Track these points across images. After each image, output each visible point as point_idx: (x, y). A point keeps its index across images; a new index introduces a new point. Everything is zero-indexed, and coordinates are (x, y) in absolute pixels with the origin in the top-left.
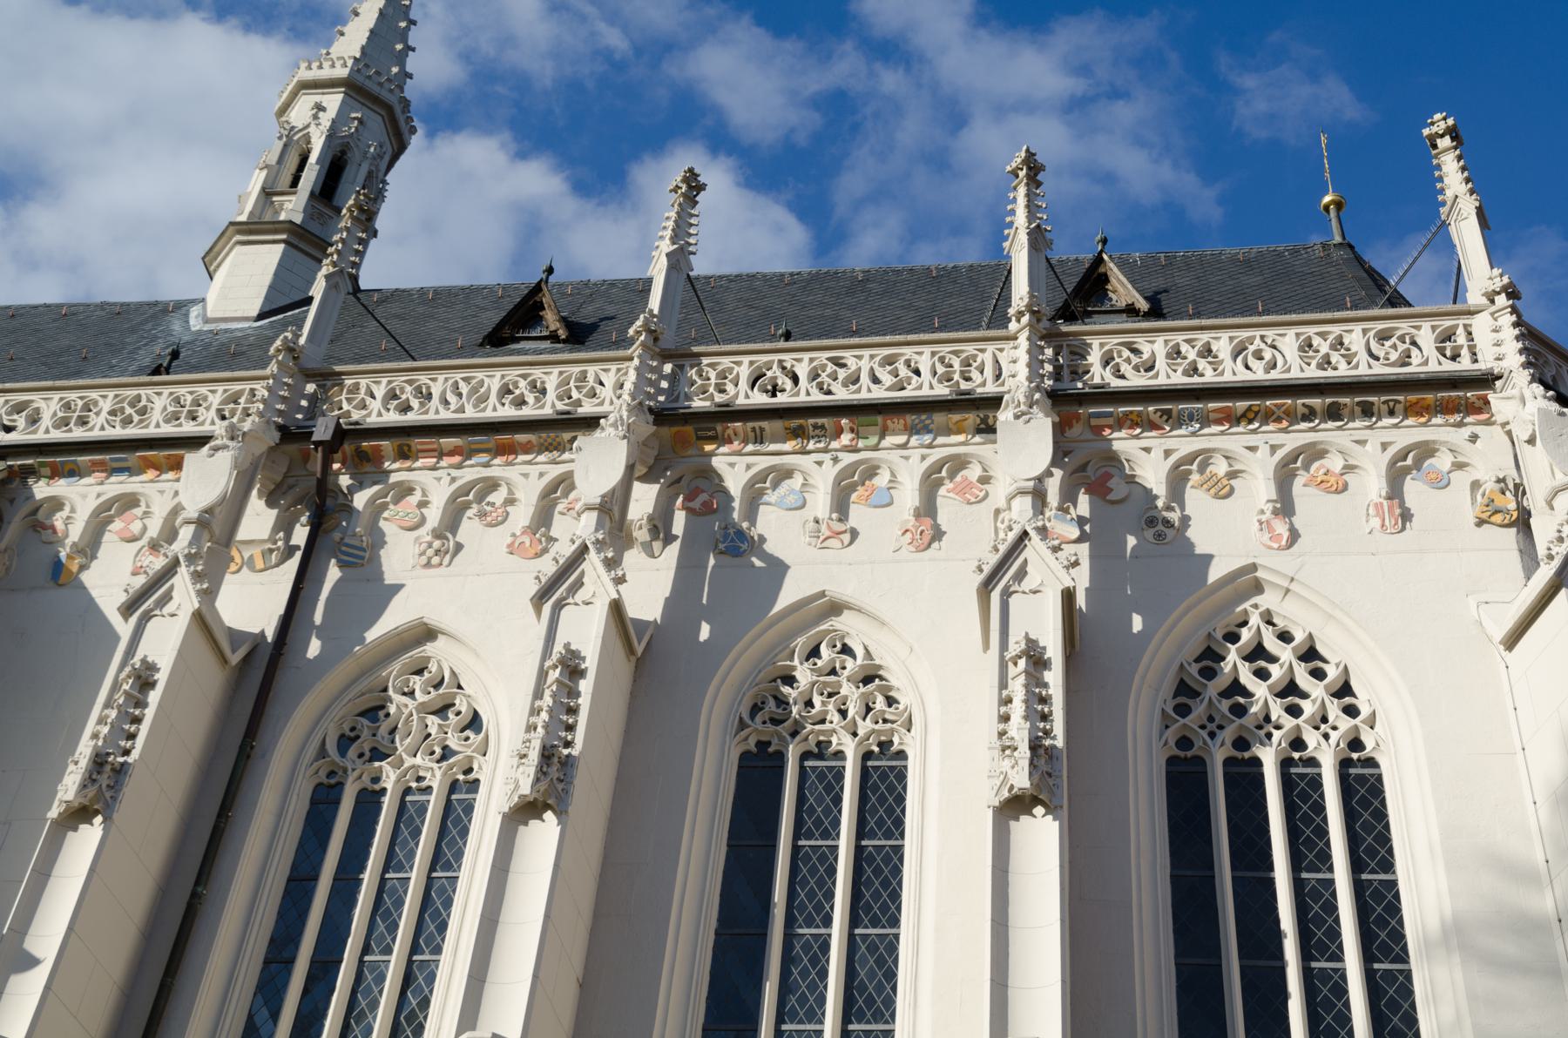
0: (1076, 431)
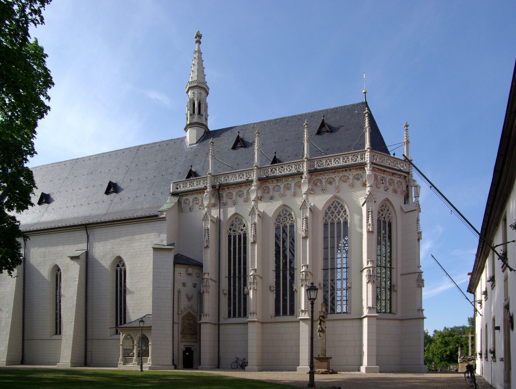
0: (313, 176)
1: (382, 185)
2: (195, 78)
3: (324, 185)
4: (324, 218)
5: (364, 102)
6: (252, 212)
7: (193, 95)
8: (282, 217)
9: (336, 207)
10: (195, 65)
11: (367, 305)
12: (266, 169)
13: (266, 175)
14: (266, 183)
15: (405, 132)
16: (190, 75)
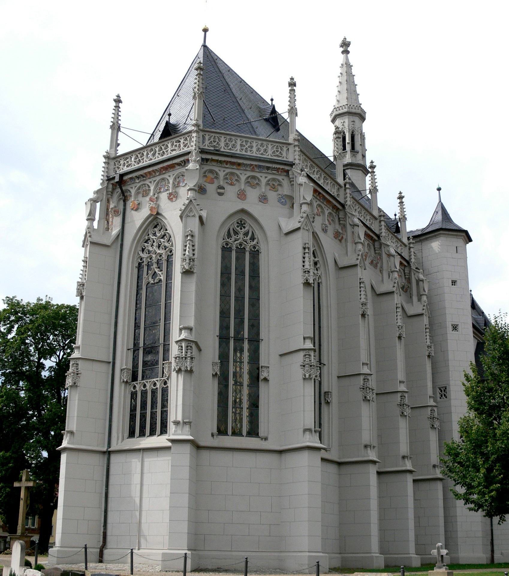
2: (345, 102)
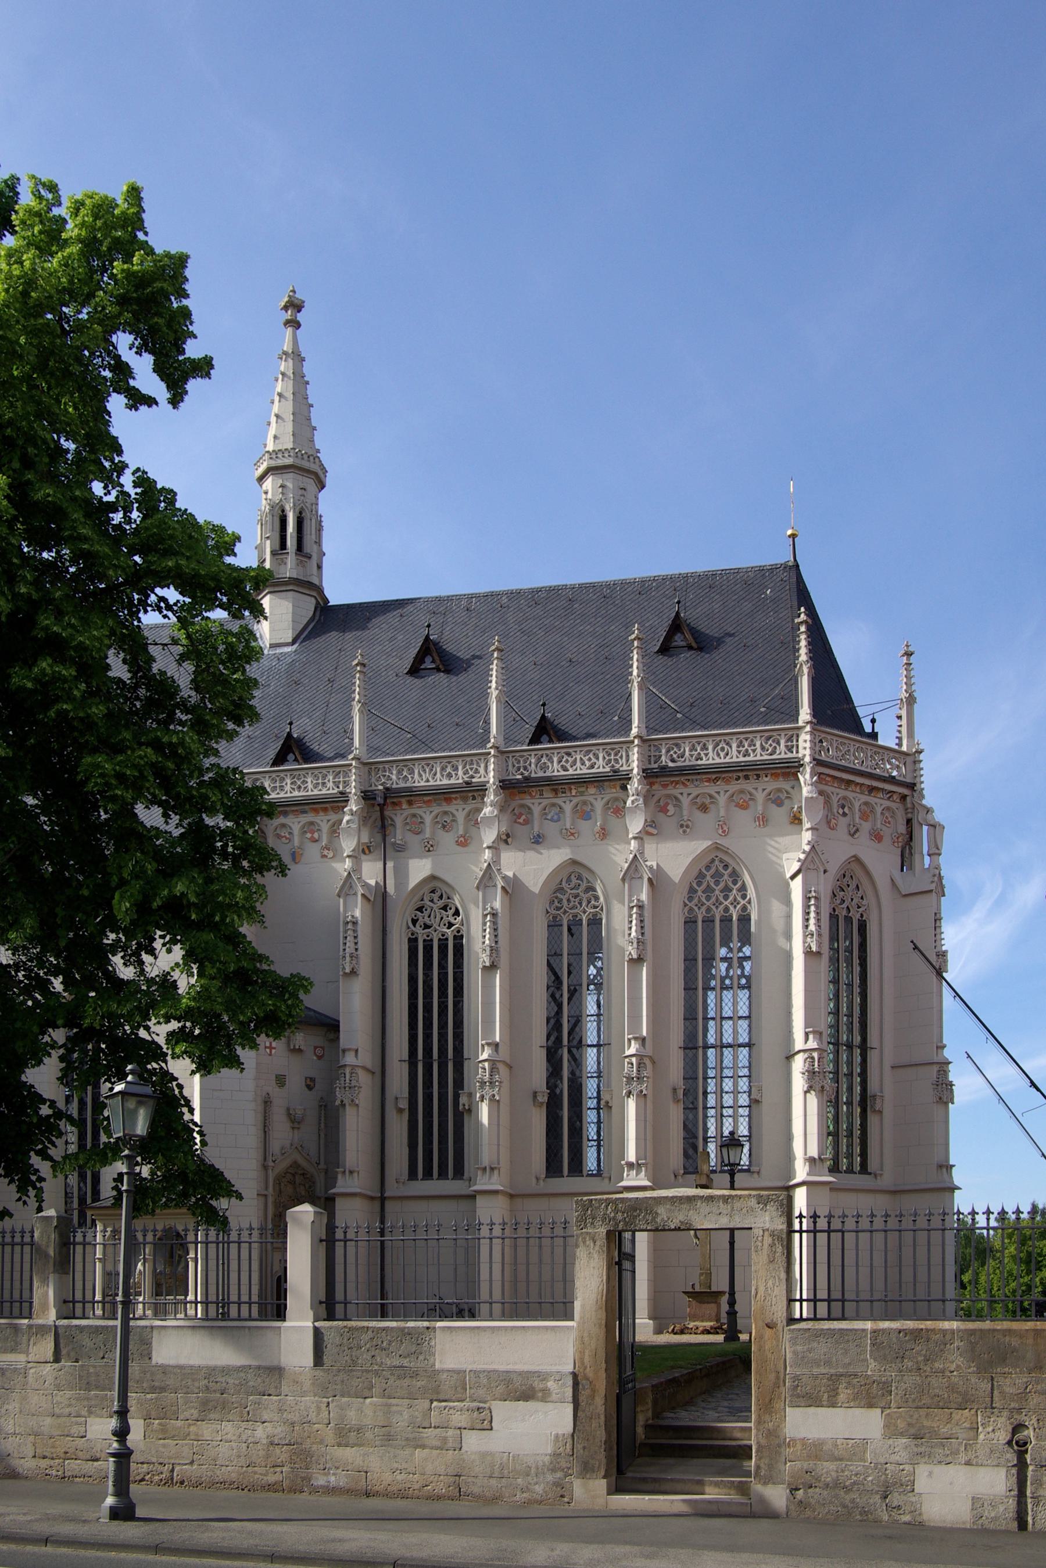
1: (840, 817)
3: (685, 813)
4: (685, 905)
5: (790, 564)
6: (487, 879)
7: (283, 493)
8: (567, 896)
9: (717, 876)
10: (286, 398)
11: (806, 1154)
12: (522, 756)
13: (522, 774)
14: (522, 796)
15: (905, 672)
16: (269, 424)
